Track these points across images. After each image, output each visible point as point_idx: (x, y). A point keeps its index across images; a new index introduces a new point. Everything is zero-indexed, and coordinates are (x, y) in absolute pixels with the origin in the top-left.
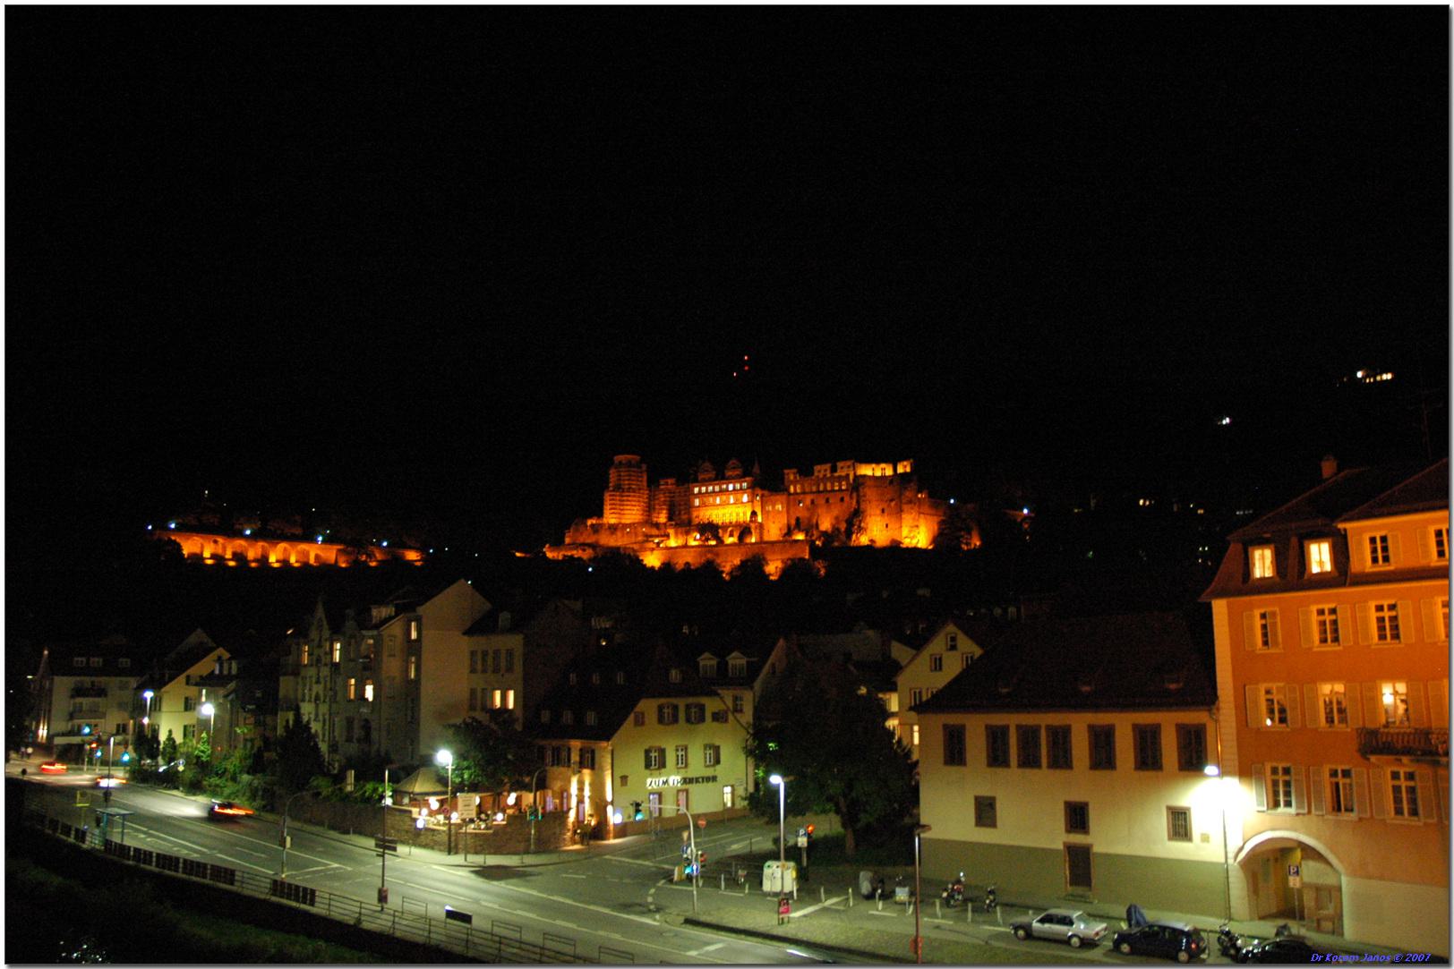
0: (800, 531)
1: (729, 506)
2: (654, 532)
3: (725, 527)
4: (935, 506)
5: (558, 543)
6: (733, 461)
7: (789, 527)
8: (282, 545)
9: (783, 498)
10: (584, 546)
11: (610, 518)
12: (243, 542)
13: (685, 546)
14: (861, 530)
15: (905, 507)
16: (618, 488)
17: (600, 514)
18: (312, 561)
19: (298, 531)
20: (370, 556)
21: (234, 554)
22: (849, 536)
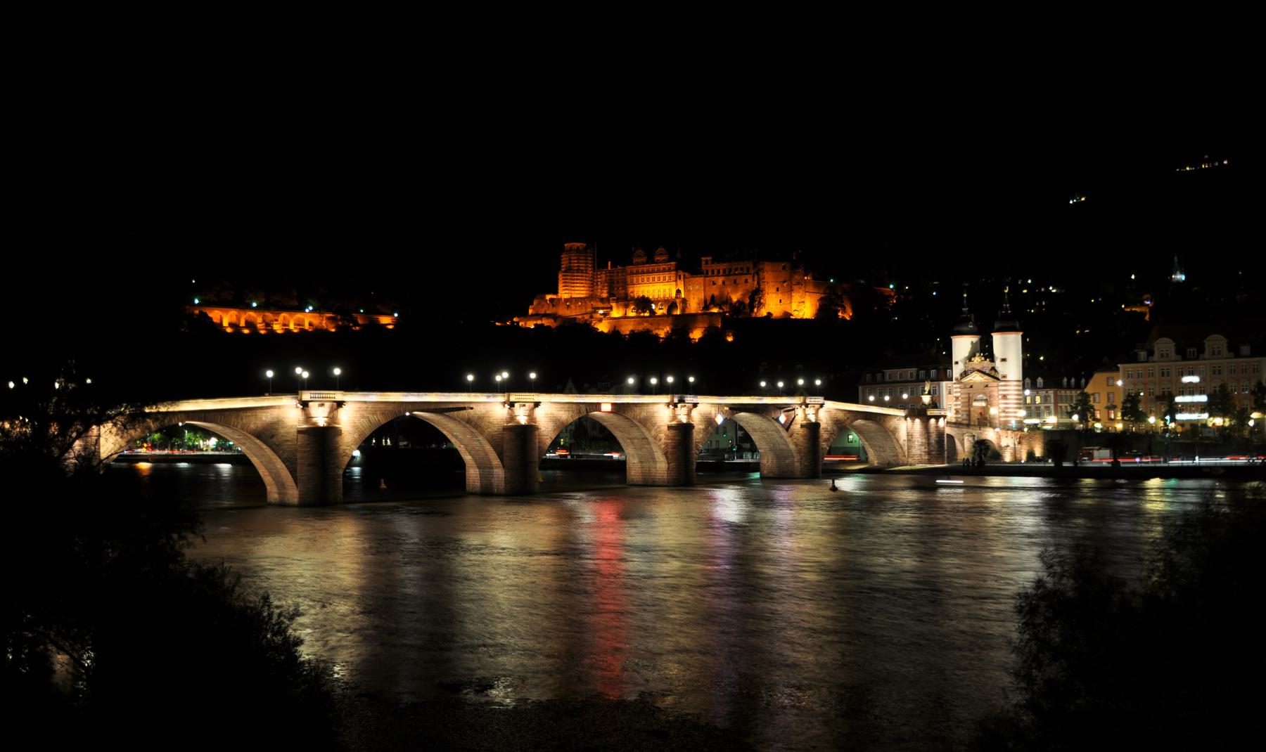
0: (716, 306)
1: (659, 288)
2: (600, 305)
3: (656, 302)
4: (816, 286)
5: (524, 314)
6: (661, 250)
7: (705, 301)
8: (283, 315)
9: (700, 280)
10: (546, 315)
11: (564, 294)
12: (252, 314)
13: (625, 317)
14: (761, 305)
15: (795, 288)
16: (569, 269)
17: (556, 292)
18: (307, 327)
19: (296, 303)
20: (356, 324)
21: (246, 322)
22: (752, 307)
